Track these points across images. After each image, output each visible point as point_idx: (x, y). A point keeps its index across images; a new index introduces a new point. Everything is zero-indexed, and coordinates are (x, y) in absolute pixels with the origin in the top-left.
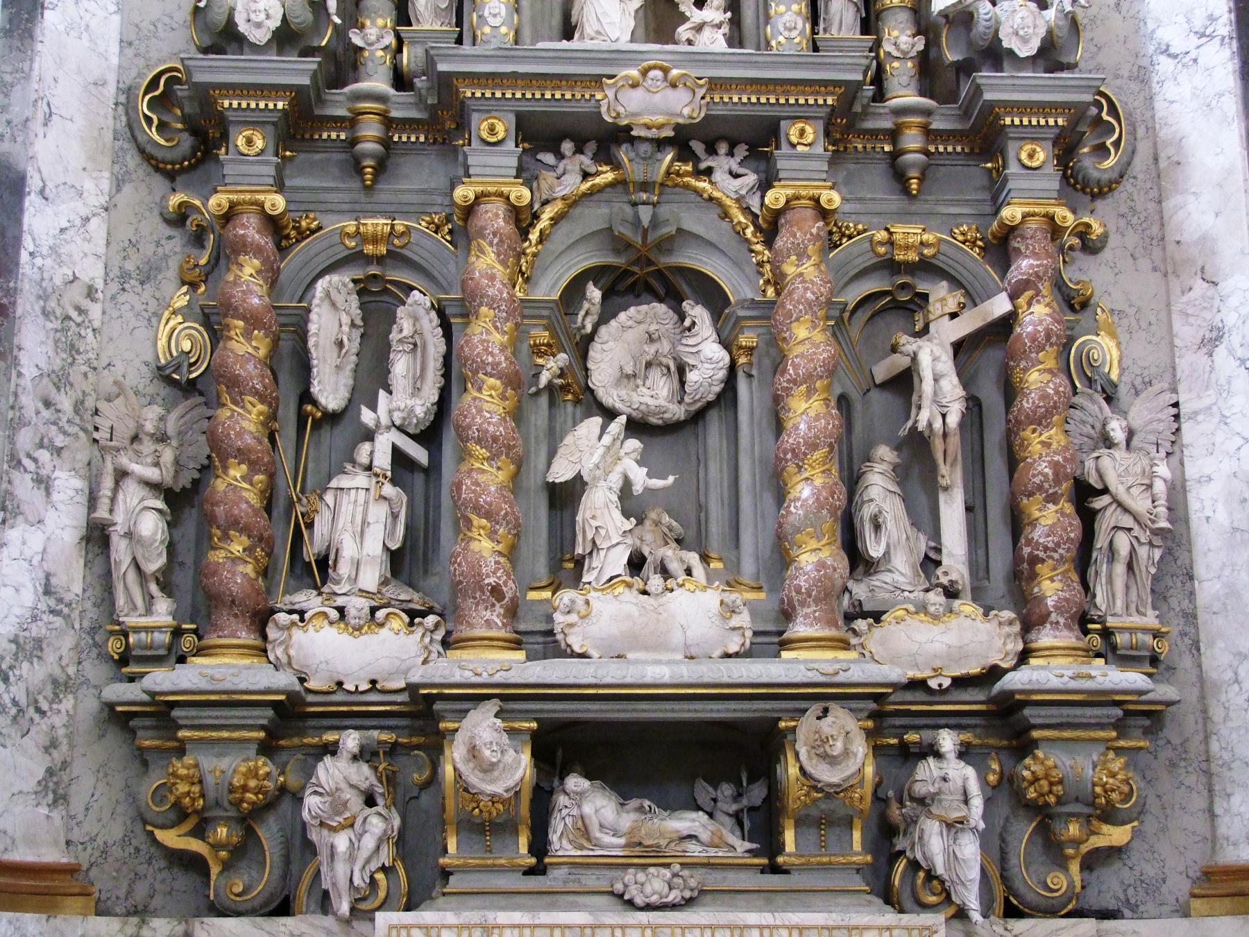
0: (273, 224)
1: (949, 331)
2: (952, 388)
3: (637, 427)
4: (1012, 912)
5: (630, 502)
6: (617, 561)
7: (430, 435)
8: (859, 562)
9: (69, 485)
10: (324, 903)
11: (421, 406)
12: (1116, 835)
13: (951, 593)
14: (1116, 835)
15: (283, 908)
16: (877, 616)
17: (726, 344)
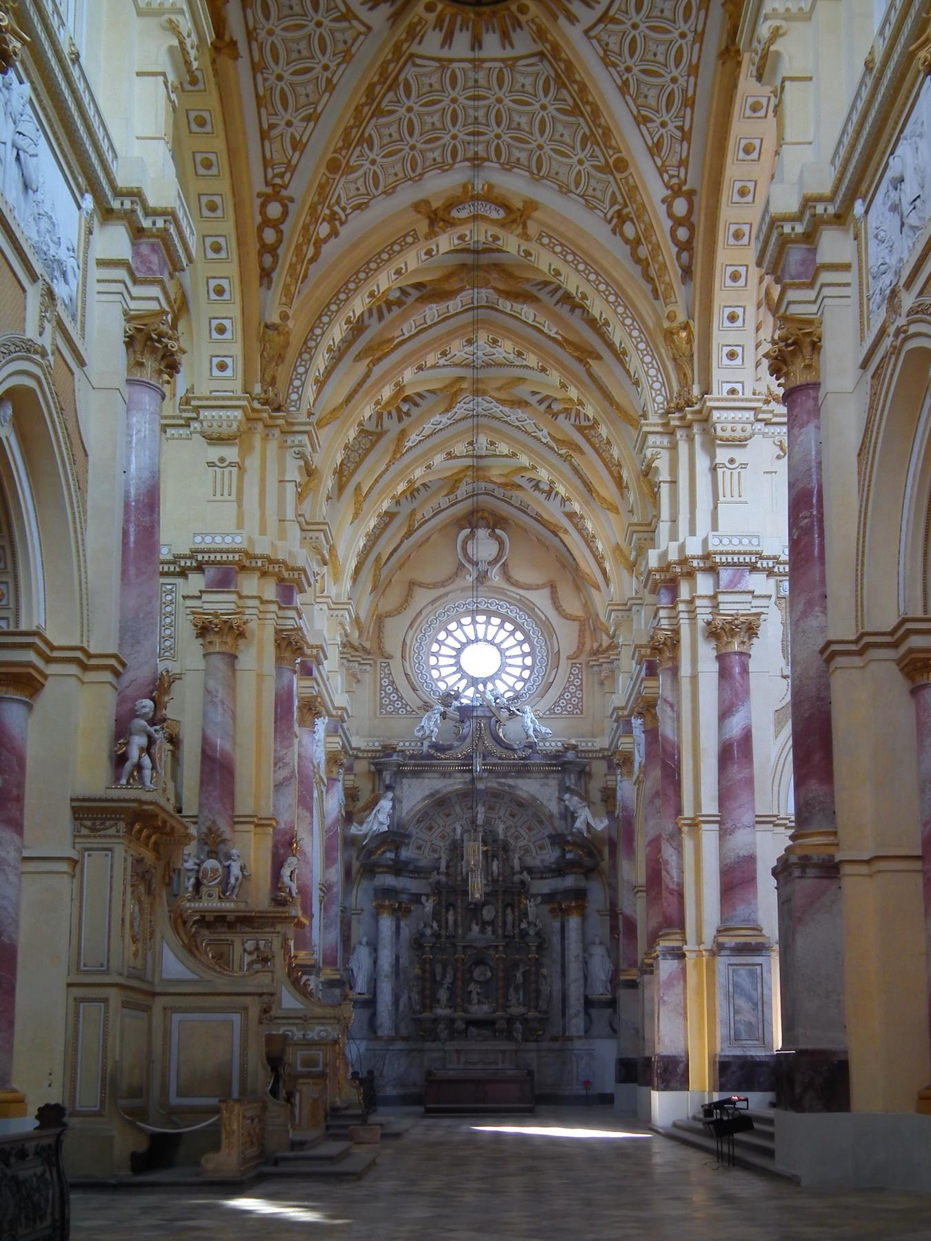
0: (431, 960)
1: (522, 970)
2: (521, 978)
3: (479, 982)
4: (527, 1041)
5: (478, 994)
6: (475, 1001)
7: (451, 984)
8: (508, 1000)
9: (406, 992)
10: (440, 1040)
11: (451, 981)
12: (540, 1033)
13: (519, 1004)
14: (540, 1033)
15: (434, 1041)
16: (509, 1007)
17: (491, 972)
